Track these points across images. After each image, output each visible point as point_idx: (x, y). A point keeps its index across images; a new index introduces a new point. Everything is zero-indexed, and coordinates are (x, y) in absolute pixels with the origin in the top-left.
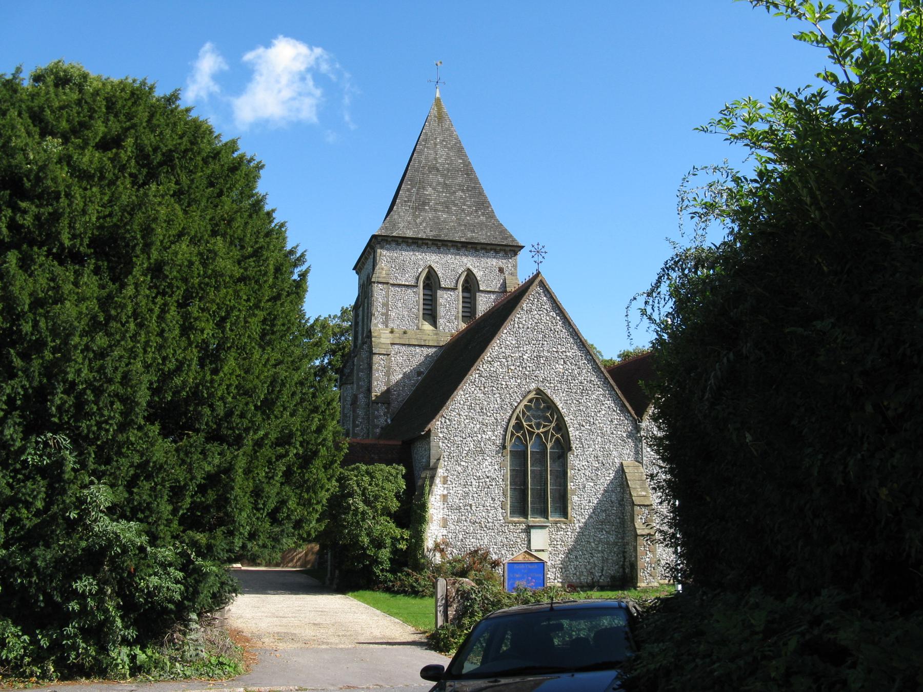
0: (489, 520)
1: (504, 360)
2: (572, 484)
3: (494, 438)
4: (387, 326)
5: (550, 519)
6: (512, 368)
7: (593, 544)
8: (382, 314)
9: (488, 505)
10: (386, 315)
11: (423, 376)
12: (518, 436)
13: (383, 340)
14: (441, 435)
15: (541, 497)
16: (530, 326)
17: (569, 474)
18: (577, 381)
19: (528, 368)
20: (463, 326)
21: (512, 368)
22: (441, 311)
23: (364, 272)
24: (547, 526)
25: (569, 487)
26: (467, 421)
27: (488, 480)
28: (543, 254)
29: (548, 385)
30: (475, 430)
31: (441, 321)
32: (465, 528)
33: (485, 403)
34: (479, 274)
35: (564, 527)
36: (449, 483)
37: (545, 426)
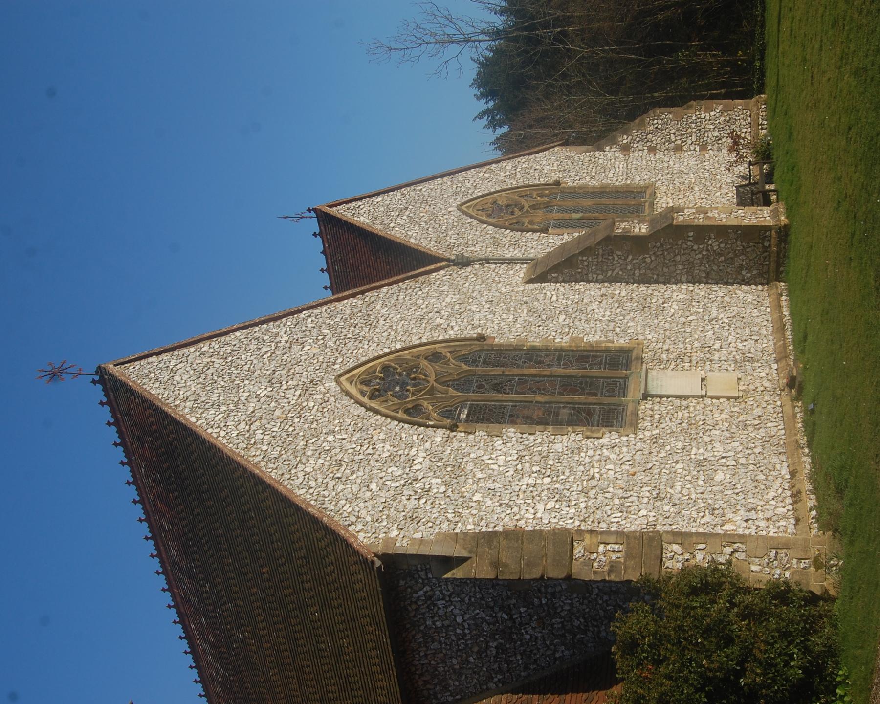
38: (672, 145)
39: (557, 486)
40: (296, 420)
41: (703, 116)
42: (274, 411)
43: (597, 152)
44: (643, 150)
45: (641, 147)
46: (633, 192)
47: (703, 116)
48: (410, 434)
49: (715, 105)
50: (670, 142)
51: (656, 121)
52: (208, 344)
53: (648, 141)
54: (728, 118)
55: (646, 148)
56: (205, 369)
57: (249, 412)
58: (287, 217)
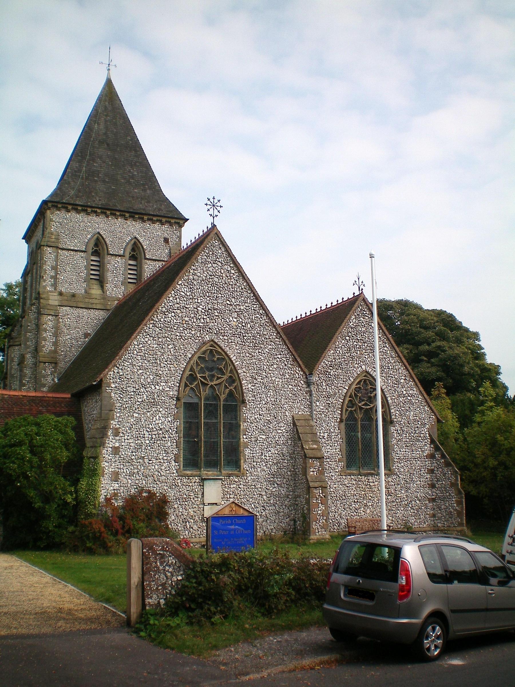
0: (162, 474)
1: (179, 311)
2: (245, 437)
3: (168, 389)
4: (55, 289)
5: (224, 472)
6: (187, 319)
7: (265, 497)
8: (52, 277)
9: (161, 457)
10: (55, 278)
11: (90, 338)
12: (192, 388)
13: (51, 302)
14: (113, 386)
15: (212, 448)
16: (204, 278)
17: (242, 427)
18: (250, 335)
19: (202, 321)
20: (131, 288)
21: (187, 319)
22: (109, 276)
23: (34, 240)
24: (222, 479)
25: (242, 440)
26: (141, 371)
27: (161, 432)
28: (219, 208)
29: (221, 337)
30: (149, 380)
31: (109, 287)
32: (137, 482)
33: (159, 353)
34: (145, 244)
35: (236, 480)
36: (122, 435)
37: (218, 378)
39: (144, 447)
40: (181, 329)
42: (188, 317)
43: (429, 440)
48: (174, 382)
52: (236, 271)
56: (217, 276)
57: (186, 306)
58: (359, 279)
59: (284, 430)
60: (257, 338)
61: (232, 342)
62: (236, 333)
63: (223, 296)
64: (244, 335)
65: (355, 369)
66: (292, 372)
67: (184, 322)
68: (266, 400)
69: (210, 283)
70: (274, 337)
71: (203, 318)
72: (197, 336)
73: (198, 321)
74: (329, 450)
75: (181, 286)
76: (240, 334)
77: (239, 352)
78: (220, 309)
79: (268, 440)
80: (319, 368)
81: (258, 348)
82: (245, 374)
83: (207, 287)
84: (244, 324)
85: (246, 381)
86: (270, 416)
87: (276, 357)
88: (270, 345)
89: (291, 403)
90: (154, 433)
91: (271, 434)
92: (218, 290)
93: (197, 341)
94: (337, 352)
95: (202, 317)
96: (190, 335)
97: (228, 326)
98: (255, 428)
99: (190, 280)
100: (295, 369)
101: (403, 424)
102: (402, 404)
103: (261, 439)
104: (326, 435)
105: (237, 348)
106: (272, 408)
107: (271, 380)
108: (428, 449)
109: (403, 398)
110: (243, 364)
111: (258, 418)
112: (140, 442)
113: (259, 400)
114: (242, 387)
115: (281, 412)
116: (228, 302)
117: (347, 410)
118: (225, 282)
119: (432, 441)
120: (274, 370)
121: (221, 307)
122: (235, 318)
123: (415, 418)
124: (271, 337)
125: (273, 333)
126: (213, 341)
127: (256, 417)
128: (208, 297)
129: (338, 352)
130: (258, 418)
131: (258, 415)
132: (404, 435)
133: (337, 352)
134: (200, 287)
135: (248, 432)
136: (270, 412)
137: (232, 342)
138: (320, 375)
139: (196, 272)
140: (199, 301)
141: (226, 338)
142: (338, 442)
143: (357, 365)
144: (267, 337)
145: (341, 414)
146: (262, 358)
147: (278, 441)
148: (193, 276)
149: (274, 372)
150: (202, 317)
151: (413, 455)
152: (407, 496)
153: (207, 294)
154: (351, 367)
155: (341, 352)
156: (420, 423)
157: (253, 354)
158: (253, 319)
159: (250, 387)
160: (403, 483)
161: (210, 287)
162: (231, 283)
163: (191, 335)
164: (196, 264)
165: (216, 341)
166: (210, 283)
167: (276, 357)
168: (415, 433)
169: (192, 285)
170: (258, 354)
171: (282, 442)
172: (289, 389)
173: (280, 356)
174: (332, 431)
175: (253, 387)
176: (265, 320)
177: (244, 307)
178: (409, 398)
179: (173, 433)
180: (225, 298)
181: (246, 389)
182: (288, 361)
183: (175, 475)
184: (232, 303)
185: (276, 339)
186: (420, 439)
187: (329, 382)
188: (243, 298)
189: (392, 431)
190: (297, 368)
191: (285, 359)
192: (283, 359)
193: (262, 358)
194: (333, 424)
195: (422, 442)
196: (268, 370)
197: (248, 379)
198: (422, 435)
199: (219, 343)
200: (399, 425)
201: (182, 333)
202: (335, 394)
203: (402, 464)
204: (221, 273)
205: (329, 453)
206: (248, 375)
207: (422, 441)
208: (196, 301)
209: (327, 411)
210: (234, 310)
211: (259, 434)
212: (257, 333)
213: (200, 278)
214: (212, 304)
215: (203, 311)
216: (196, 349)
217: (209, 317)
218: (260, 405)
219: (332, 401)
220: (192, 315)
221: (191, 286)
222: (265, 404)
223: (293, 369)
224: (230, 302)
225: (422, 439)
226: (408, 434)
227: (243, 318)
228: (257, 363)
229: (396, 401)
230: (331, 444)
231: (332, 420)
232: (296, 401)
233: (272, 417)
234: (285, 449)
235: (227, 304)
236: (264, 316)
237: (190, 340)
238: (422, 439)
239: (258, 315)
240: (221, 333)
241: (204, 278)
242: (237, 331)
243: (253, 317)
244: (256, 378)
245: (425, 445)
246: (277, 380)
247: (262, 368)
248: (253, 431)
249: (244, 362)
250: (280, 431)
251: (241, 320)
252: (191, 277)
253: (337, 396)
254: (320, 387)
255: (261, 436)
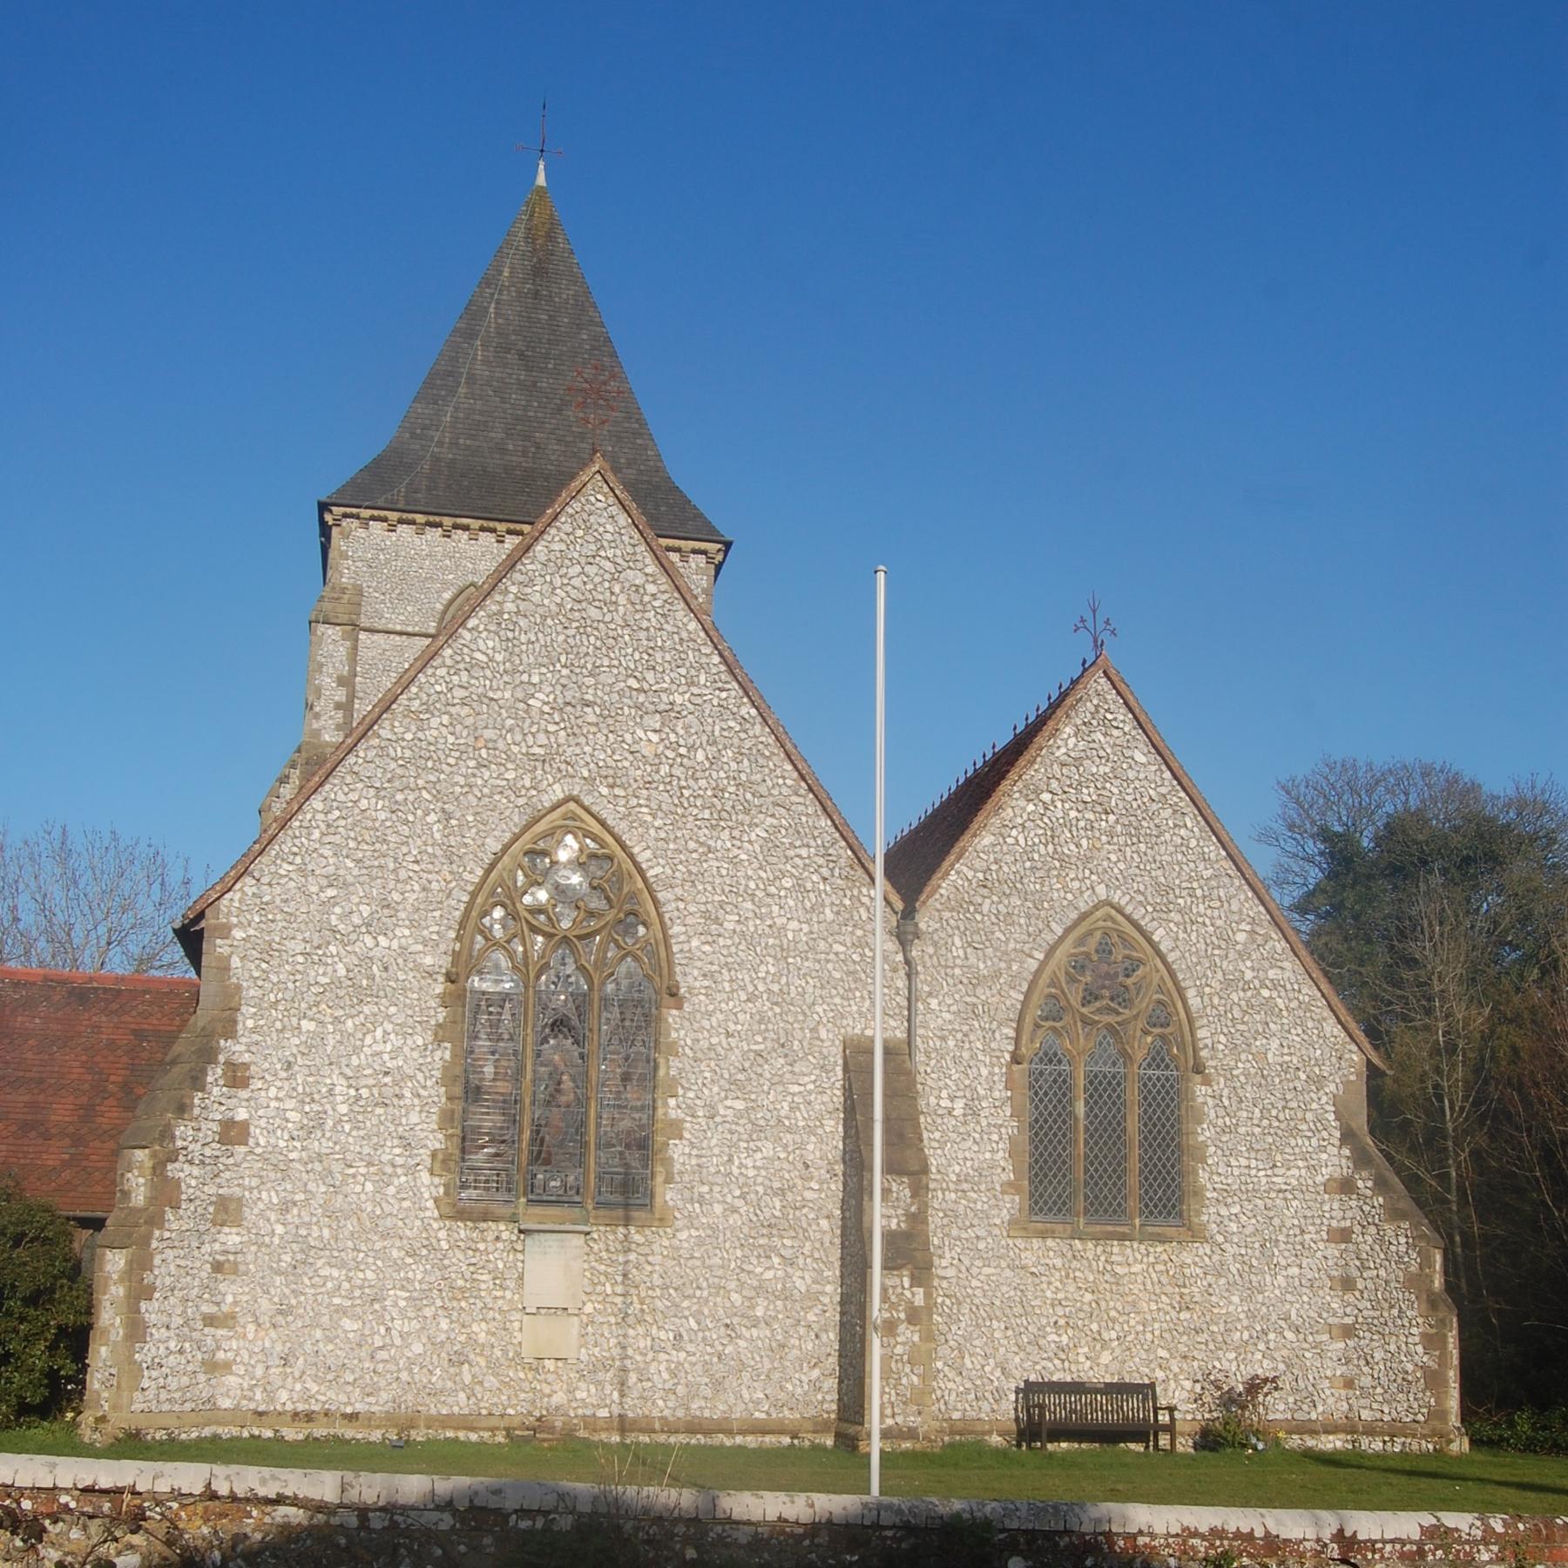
2: (672, 1102)
18: (703, 783)
25: (660, 1112)
27: (388, 1080)
29: (605, 791)
38: (1355, 1273)
41: (1414, 1330)
44: (1344, 1218)
45: (1349, 1214)
46: (1181, 1203)
47: (1414, 1330)
49: (1437, 1353)
50: (1363, 1268)
51: (1403, 1240)
53: (1364, 1227)
54: (1410, 1378)
55: (1348, 1223)
56: (597, 603)
59: (811, 1086)
60: (727, 795)
61: (641, 806)
62: (656, 777)
63: (615, 663)
64: (683, 783)
65: (1070, 896)
66: (847, 902)
67: (481, 744)
68: (750, 988)
69: (575, 624)
70: (785, 791)
71: (547, 731)
72: (523, 786)
73: (530, 739)
74: (967, 1155)
75: (476, 634)
76: (668, 780)
77: (663, 835)
78: (603, 706)
79: (752, 1116)
80: (942, 891)
81: (730, 824)
82: (681, 905)
83: (561, 638)
84: (683, 751)
85: (684, 929)
86: (765, 1039)
87: (791, 853)
88: (773, 816)
89: (837, 1000)
90: (363, 1082)
91: (764, 1096)
92: (599, 643)
93: (521, 801)
94: (1008, 840)
95: (543, 727)
96: (498, 782)
97: (627, 755)
98: (707, 1074)
99: (506, 616)
100: (855, 892)
101: (1242, 1079)
102: (1237, 1013)
103: (729, 1112)
104: (959, 1105)
105: (658, 823)
106: (770, 1013)
107: (770, 926)
108: (1334, 1161)
109: (1241, 994)
110: (677, 874)
111: (720, 1043)
112: (316, 1107)
113: (728, 989)
114: (668, 947)
115: (802, 1029)
116: (633, 683)
117: (1037, 1026)
118: (625, 621)
119: (1348, 1136)
120: (782, 893)
121: (606, 698)
122: (655, 731)
123: (1287, 1058)
124: (775, 792)
125: (784, 778)
126: (576, 800)
127: (714, 1040)
128: (565, 666)
129: (1010, 840)
130: (720, 1043)
131: (723, 1037)
132: (1245, 1114)
133: (1008, 840)
134: (540, 635)
135: (683, 1087)
136: (763, 1027)
137: (641, 806)
138: (947, 915)
139: (528, 590)
140: (535, 679)
141: (622, 793)
142: (1003, 1130)
143: (1076, 884)
144: (763, 790)
145: (1017, 1040)
146: (744, 857)
147: (788, 1118)
148: (519, 601)
149: (783, 901)
150: (543, 727)
151: (1275, 1179)
152: (1251, 1315)
153: (563, 659)
154: (1058, 890)
155: (1022, 842)
156: (1303, 1077)
157: (711, 843)
158: (717, 733)
159: (697, 948)
160: (1235, 1272)
161: (574, 636)
162: (645, 624)
163: (505, 783)
164: (529, 567)
165: (587, 801)
166: (575, 624)
167: (791, 853)
168: (1284, 1108)
169: (513, 631)
170: (729, 845)
171: (801, 1124)
172: (832, 956)
173: (804, 852)
174: (982, 1092)
175: (707, 948)
176: (755, 737)
177: (687, 696)
178: (1266, 993)
179: (429, 1083)
180: (621, 669)
181: (681, 951)
182: (831, 865)
183: (428, 1214)
184: (646, 686)
185: (794, 799)
186: (1304, 1127)
187: (977, 938)
188: (683, 671)
189: (1200, 1100)
190: (864, 890)
191: (821, 861)
192: (816, 859)
193: (744, 857)
194: (984, 1072)
195: (1309, 1138)
196: (760, 894)
197: (689, 920)
198: (1309, 1116)
199: (595, 809)
200: (1226, 1079)
201: (474, 776)
202: (997, 974)
203: (1235, 1209)
204: (612, 593)
205: (969, 1164)
206: (692, 909)
207: (1310, 1134)
208: (525, 677)
209: (965, 1028)
210: (652, 708)
211: (723, 1094)
212: (727, 777)
213: (540, 610)
214: (579, 687)
215: (546, 709)
216: (516, 825)
217: (565, 728)
218: (731, 1003)
219: (983, 997)
220: (510, 722)
221: (510, 635)
222: (748, 1000)
223: (849, 893)
224: (638, 681)
225: (1310, 1130)
226: (1257, 1111)
227: (681, 732)
228: (724, 872)
229: (1216, 1001)
230: (977, 1136)
231: (980, 1057)
232: (858, 994)
233: (769, 1044)
234: (811, 1147)
235: (629, 687)
236: (754, 725)
237: (497, 797)
238: (1310, 1130)
239: (732, 724)
240: (606, 777)
241: (554, 608)
242: (657, 772)
243: (717, 728)
244: (717, 918)
245: (1322, 1149)
246: (794, 925)
247: (742, 888)
248: (704, 1084)
249: (680, 867)
250: (796, 1089)
251: (673, 737)
252: (509, 606)
253: (1002, 981)
254: (943, 951)
255: (728, 1103)
